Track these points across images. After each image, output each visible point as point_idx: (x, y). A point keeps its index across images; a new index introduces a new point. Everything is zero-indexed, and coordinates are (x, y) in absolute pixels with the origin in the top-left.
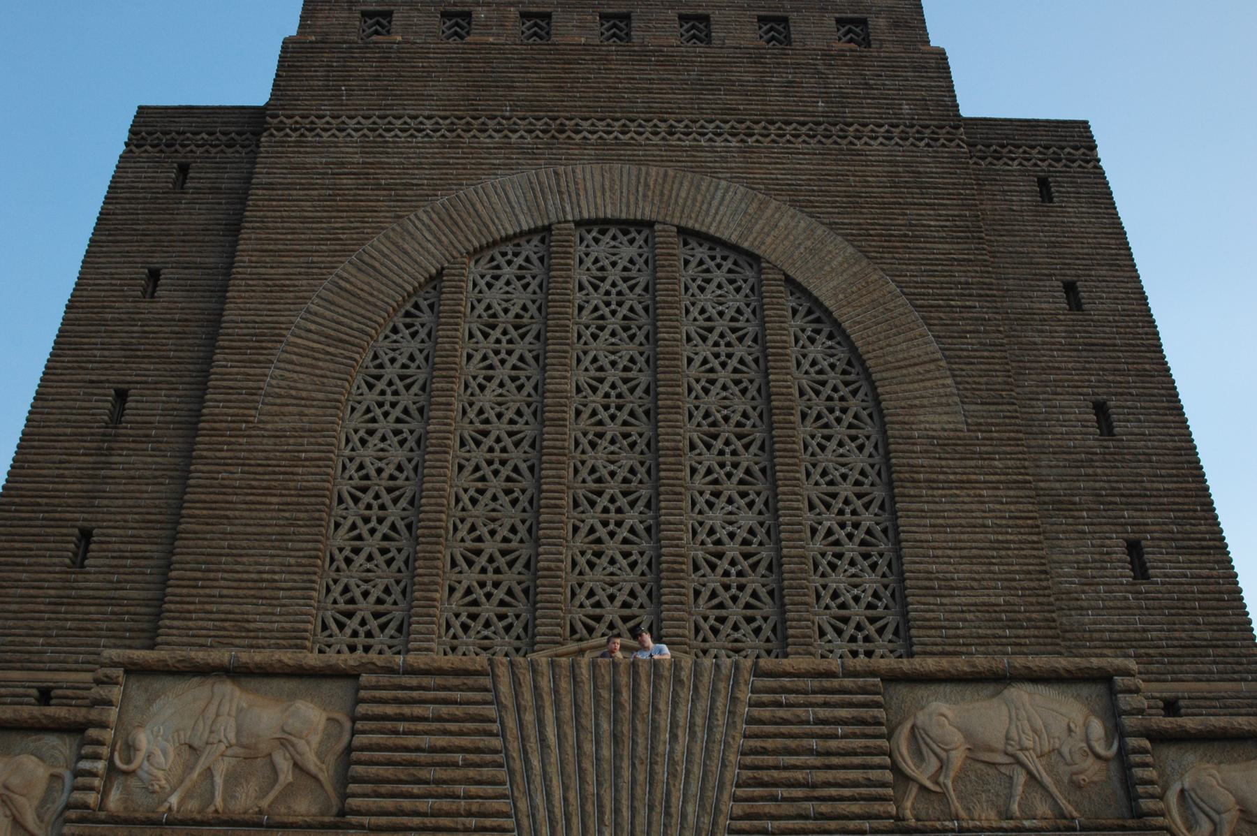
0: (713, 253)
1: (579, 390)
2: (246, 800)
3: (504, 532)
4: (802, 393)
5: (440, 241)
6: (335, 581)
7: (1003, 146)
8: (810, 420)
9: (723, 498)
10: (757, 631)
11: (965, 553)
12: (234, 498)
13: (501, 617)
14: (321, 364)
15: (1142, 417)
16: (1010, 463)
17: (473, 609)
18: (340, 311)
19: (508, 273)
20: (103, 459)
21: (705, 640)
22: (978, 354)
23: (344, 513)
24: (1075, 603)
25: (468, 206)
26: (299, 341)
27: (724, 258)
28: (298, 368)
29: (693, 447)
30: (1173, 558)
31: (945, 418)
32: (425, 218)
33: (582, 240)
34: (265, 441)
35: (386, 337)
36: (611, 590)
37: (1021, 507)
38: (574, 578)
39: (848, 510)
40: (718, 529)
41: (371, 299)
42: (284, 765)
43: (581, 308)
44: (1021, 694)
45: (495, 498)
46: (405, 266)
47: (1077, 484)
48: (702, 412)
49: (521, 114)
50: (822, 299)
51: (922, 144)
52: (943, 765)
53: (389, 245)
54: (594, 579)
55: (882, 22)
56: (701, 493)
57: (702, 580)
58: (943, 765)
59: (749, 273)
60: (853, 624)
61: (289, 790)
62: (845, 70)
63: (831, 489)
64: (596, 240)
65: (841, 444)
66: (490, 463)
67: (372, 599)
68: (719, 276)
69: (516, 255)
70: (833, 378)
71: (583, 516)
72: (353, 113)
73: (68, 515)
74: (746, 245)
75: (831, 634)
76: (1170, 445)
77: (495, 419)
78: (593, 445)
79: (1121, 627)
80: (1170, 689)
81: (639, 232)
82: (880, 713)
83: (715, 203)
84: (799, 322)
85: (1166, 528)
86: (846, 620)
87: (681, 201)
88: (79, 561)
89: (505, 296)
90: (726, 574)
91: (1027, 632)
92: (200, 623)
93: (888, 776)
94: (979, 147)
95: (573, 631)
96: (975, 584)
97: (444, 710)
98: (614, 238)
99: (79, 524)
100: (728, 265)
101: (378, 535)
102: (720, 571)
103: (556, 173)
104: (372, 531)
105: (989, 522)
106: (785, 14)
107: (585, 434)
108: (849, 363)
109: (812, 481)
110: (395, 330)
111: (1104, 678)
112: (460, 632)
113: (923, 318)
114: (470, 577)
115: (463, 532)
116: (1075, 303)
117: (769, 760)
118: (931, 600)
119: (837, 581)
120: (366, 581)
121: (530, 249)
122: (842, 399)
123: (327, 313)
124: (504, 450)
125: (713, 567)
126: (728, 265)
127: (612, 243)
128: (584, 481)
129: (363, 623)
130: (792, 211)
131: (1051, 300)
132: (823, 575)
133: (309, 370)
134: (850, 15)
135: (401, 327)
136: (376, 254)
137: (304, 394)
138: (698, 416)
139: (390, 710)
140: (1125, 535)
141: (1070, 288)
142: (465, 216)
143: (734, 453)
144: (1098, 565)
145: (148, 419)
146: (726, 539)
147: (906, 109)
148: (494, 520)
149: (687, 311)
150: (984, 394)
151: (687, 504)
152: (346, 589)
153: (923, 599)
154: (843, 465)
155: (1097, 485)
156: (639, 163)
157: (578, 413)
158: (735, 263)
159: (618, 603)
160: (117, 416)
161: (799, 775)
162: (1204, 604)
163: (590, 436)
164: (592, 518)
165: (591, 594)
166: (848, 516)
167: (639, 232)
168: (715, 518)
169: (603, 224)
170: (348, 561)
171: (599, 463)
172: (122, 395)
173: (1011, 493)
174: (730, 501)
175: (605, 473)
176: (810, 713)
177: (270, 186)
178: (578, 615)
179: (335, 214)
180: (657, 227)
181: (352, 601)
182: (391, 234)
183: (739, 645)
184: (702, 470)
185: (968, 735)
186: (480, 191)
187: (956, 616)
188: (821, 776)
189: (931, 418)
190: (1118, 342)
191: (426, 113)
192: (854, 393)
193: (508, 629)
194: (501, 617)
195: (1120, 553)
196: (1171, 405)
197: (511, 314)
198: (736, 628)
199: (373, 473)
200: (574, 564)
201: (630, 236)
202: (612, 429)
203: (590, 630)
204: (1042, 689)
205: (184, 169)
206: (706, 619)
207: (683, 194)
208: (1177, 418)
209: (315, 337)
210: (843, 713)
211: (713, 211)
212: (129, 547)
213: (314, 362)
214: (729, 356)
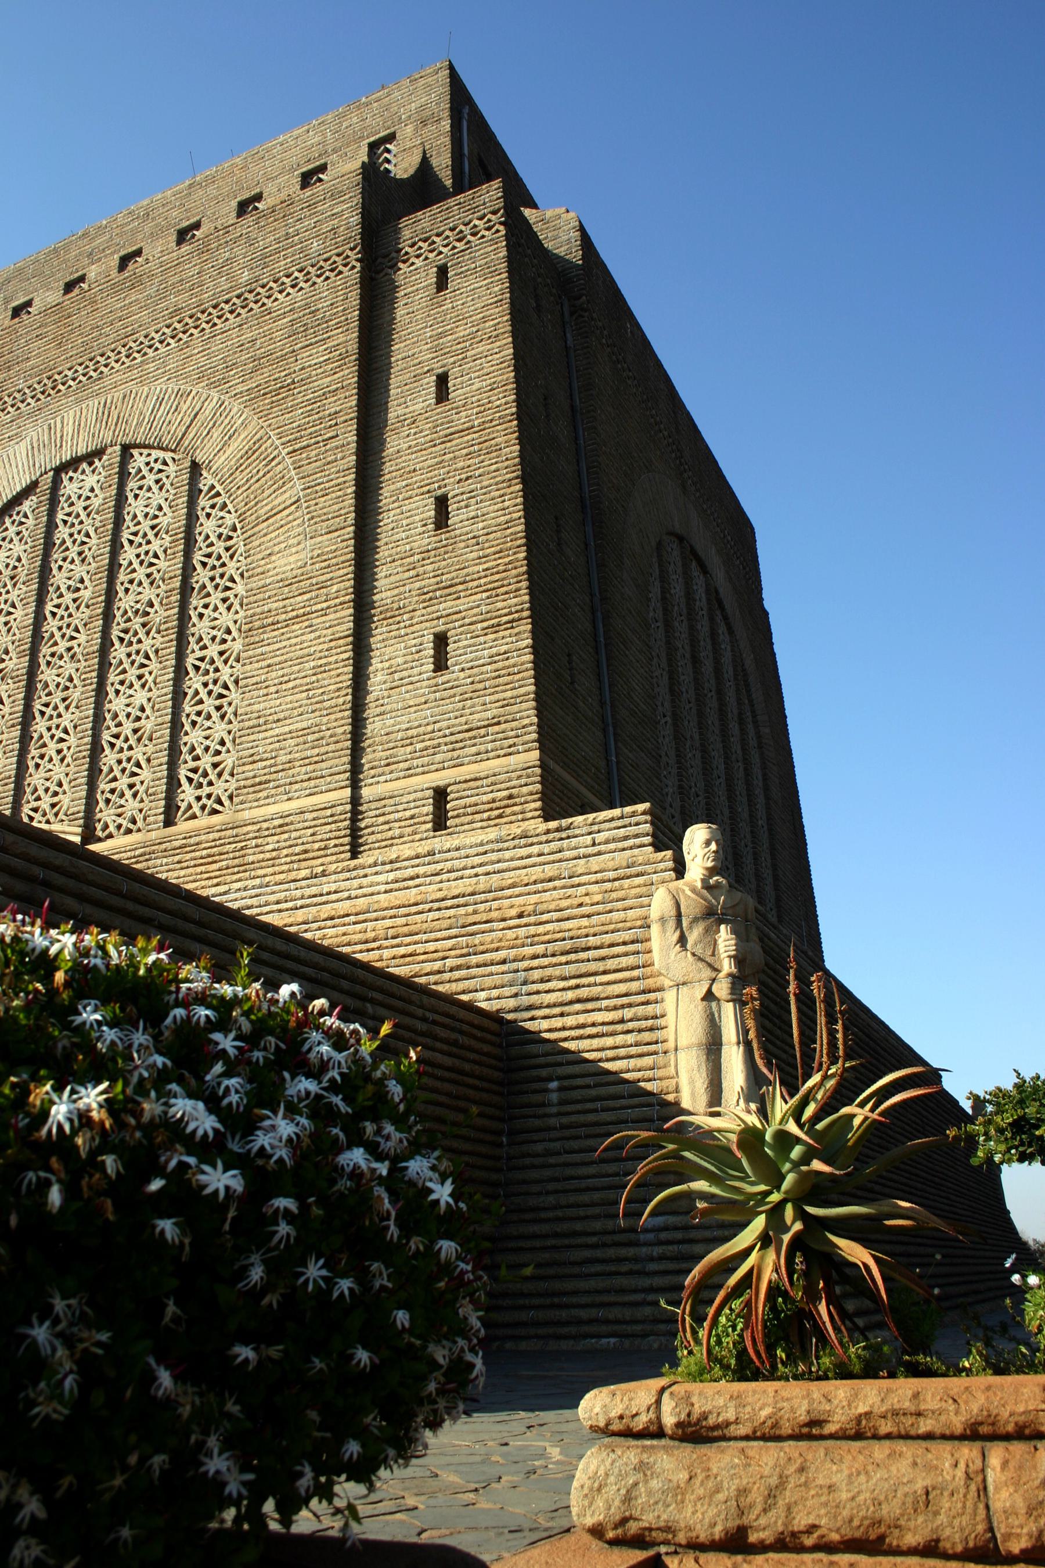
19: (12, 530)
31: (292, 559)
55: (409, 129)
69: (18, 513)
70: (219, 547)
80: (439, 779)
81: (100, 460)
85: (475, 611)
94: (394, 255)
121: (27, 506)
134: (382, 134)
141: (442, 381)
167: (100, 460)
169: (73, 464)
180: (109, 450)
189: (282, 562)
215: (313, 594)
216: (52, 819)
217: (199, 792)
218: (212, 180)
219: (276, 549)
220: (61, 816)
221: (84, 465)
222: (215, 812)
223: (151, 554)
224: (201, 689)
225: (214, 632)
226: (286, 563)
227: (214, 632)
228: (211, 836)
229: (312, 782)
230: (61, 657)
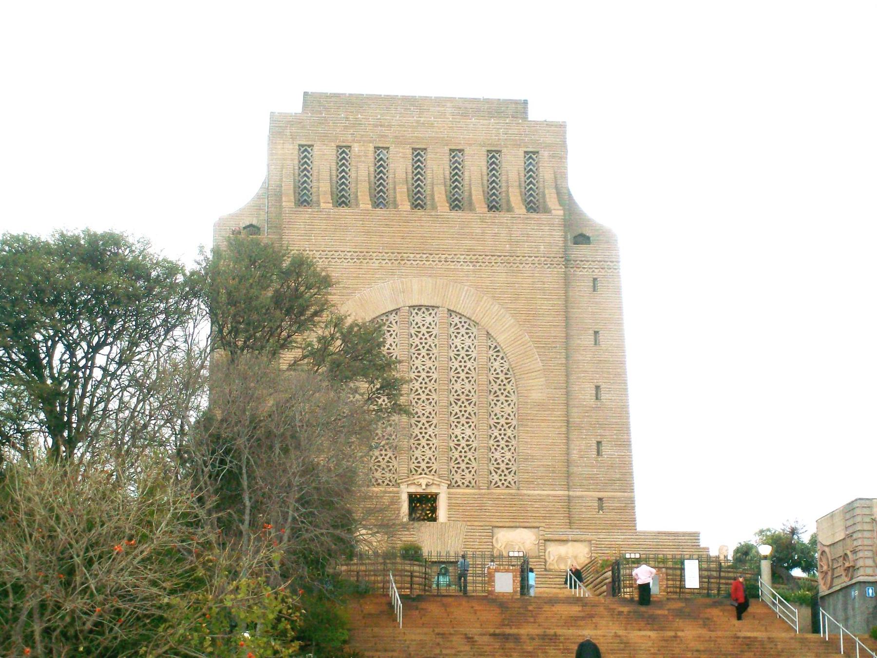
7: (582, 261)
10: (470, 472)
27: (465, 322)
31: (540, 395)
44: (519, 530)
51: (546, 266)
55: (546, 154)
59: (474, 330)
68: (463, 331)
70: (502, 376)
72: (318, 249)
80: (601, 495)
81: (433, 310)
84: (491, 352)
90: (461, 452)
94: (572, 262)
98: (424, 313)
100: (466, 326)
102: (459, 451)
108: (508, 370)
122: (504, 385)
126: (466, 326)
131: (589, 340)
141: (596, 333)
143: (465, 406)
158: (469, 325)
166: (503, 431)
167: (433, 310)
169: (419, 307)
174: (463, 425)
195: (595, 447)
203: (416, 471)
204: (525, 529)
214: (465, 367)
215: (549, 412)
216: (428, 473)
219: (533, 388)
220: (433, 472)
221: (423, 309)
222: (507, 487)
223: (467, 368)
224: (498, 436)
225: (503, 414)
226: (536, 395)
227: (503, 414)
228: (511, 497)
229: (552, 486)
230: (423, 402)
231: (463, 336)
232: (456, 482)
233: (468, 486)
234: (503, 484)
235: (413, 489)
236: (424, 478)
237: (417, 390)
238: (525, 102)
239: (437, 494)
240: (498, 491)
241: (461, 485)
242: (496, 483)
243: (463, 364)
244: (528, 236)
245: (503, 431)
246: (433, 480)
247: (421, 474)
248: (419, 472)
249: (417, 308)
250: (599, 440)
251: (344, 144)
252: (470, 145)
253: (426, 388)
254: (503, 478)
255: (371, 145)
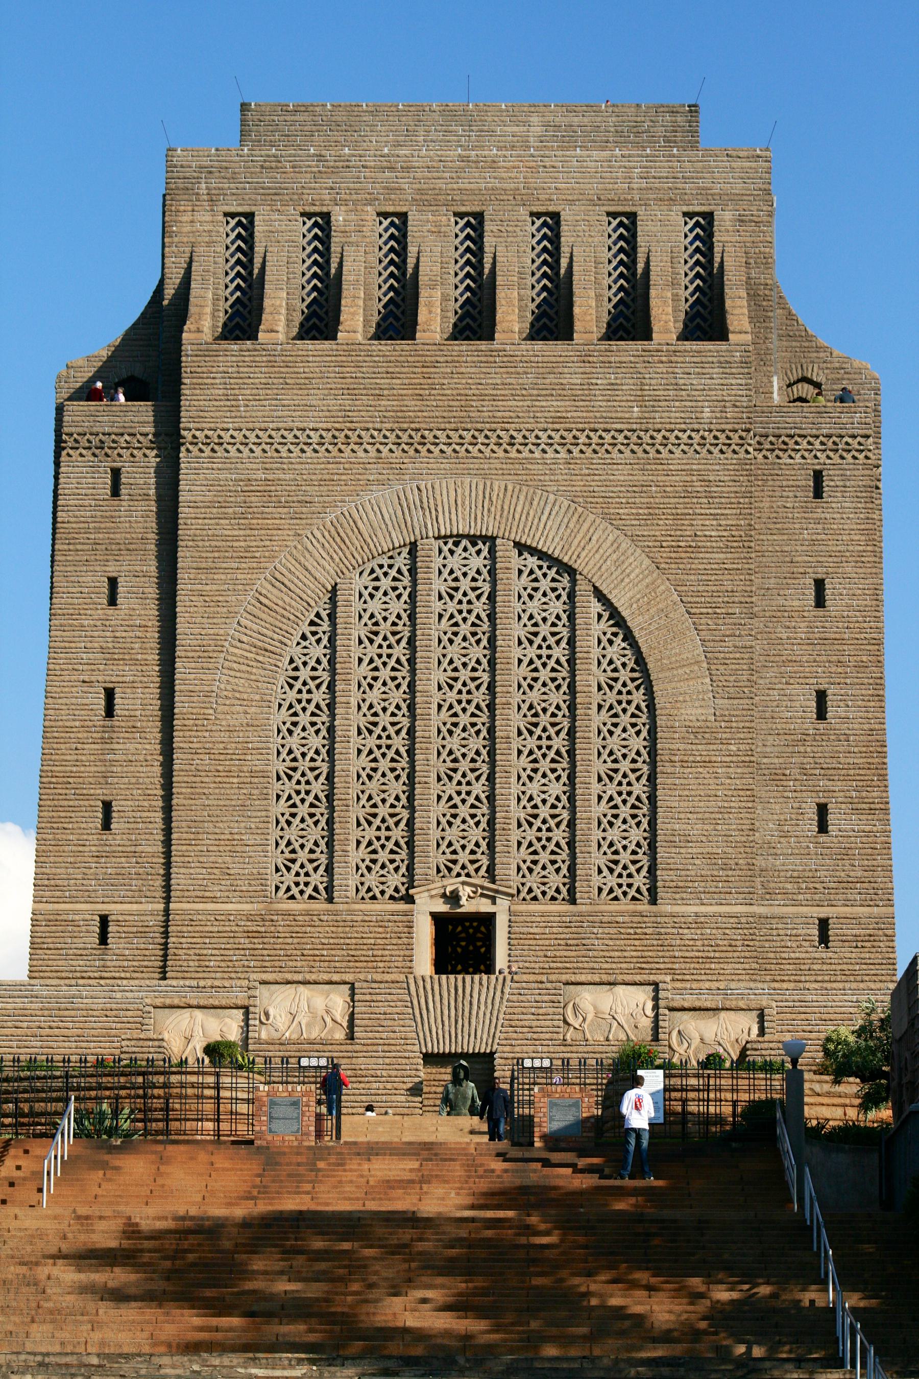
0: (540, 563)
1: (440, 688)
2: (314, 1034)
3: (391, 800)
4: (600, 688)
5: (332, 557)
6: (281, 837)
8: (604, 711)
9: (540, 773)
11: (700, 816)
12: (206, 779)
13: (392, 861)
14: (254, 670)
15: (850, 703)
16: (742, 747)
17: (374, 856)
18: (263, 623)
20: (108, 746)
21: (523, 876)
22: (731, 656)
23: (282, 787)
24: (772, 851)
25: (352, 523)
26: (236, 651)
27: (549, 568)
28: (238, 674)
29: (520, 733)
30: (848, 817)
31: (700, 711)
32: (319, 536)
33: (440, 551)
34: (222, 734)
35: (298, 644)
36: (462, 842)
37: (744, 781)
38: (438, 834)
39: (625, 781)
40: (535, 796)
41: (285, 613)
42: (328, 1020)
43: (440, 616)
44: (620, 989)
45: (384, 775)
46: (308, 582)
47: (791, 760)
48: (527, 705)
49: (388, 426)
50: (620, 609)
52: (584, 1020)
53: (294, 562)
54: (452, 834)
56: (524, 770)
57: (523, 834)
58: (584, 1020)
60: (621, 866)
61: (332, 1031)
62: (662, 368)
63: (615, 766)
64: (452, 552)
65: (624, 730)
66: (379, 747)
67: (307, 850)
68: (545, 585)
69: (390, 566)
70: (624, 675)
71: (444, 788)
72: (251, 425)
73: (92, 791)
74: (566, 560)
75: (606, 872)
76: (866, 727)
77: (381, 713)
78: (450, 732)
79: (801, 868)
80: (824, 912)
82: (561, 998)
83: (544, 518)
84: (603, 625)
85: (848, 794)
86: (616, 862)
87: (517, 516)
88: (106, 825)
89: (384, 606)
91: (734, 873)
92: (198, 870)
93: (561, 1024)
94: (771, 438)
95: (439, 871)
96: (704, 839)
97: (389, 997)
98: (465, 550)
99: (101, 798)
100: (552, 573)
101: (307, 804)
103: (419, 489)
104: (303, 801)
105: (720, 793)
106: (633, 209)
107: (445, 724)
109: (602, 760)
110: (304, 637)
111: (656, 984)
112: (365, 872)
113: (694, 624)
114: (370, 833)
115: (363, 801)
116: (820, 602)
117: (516, 1017)
118: (673, 850)
119: (614, 834)
120: (302, 837)
122: (629, 693)
123: (255, 627)
124: (389, 737)
125: (530, 824)
127: (464, 555)
128: (444, 761)
129: (302, 866)
130: (605, 524)
132: (604, 830)
133: (246, 675)
135: (309, 635)
136: (284, 571)
137: (245, 696)
138: (525, 707)
139: (368, 997)
140: (817, 800)
141: (820, 585)
142: (350, 534)
144: (794, 822)
145: (132, 713)
146: (540, 804)
147: (707, 411)
148: (384, 792)
149: (520, 618)
150: (732, 690)
151: (514, 779)
152: (289, 843)
153: (668, 850)
154: (625, 747)
155: (805, 761)
156: (485, 477)
157: (440, 706)
158: (557, 573)
159: (467, 851)
160: (110, 711)
161: (527, 1023)
162: (862, 851)
163: (448, 726)
164: (451, 789)
165: (450, 844)
166: (624, 786)
168: (533, 788)
170: (289, 823)
171: (455, 747)
172: (110, 694)
173: (739, 770)
174: (544, 776)
175: (458, 754)
176: (532, 998)
177: (194, 505)
178: (442, 860)
179: (248, 532)
181: (293, 851)
182: (294, 552)
183: (545, 880)
184: (526, 753)
185: (595, 1008)
186: (361, 508)
187: (688, 861)
188: (535, 1023)
190: (846, 636)
191: (311, 425)
192: (637, 688)
193: (397, 869)
194: (392, 861)
195: (812, 813)
196: (876, 692)
197: (389, 622)
198: (544, 868)
199: (299, 757)
200: (439, 823)
201: (477, 548)
202: (464, 719)
203: (450, 870)
205: (116, 473)
206: (524, 862)
207: (519, 509)
208: (878, 704)
209: (247, 647)
210: (546, 998)
211: (542, 525)
212: (139, 814)
213: (249, 669)
216: (473, 873)
217: (620, 881)
218: (493, 164)
221: (464, 542)
231: (545, 595)
232: (530, 891)
233: (553, 899)
234: (625, 894)
235: (442, 907)
236: (463, 883)
237: (451, 707)
238: (694, 109)
239: (493, 915)
240: (614, 907)
241: (540, 896)
242: (611, 891)
243: (544, 652)
244: (678, 387)
245: (624, 786)
246: (482, 888)
247: (459, 875)
248: (454, 873)
249: (451, 541)
250: (823, 801)
251: (317, 209)
252: (571, 202)
253: (469, 702)
254: (624, 881)
255: (369, 208)
